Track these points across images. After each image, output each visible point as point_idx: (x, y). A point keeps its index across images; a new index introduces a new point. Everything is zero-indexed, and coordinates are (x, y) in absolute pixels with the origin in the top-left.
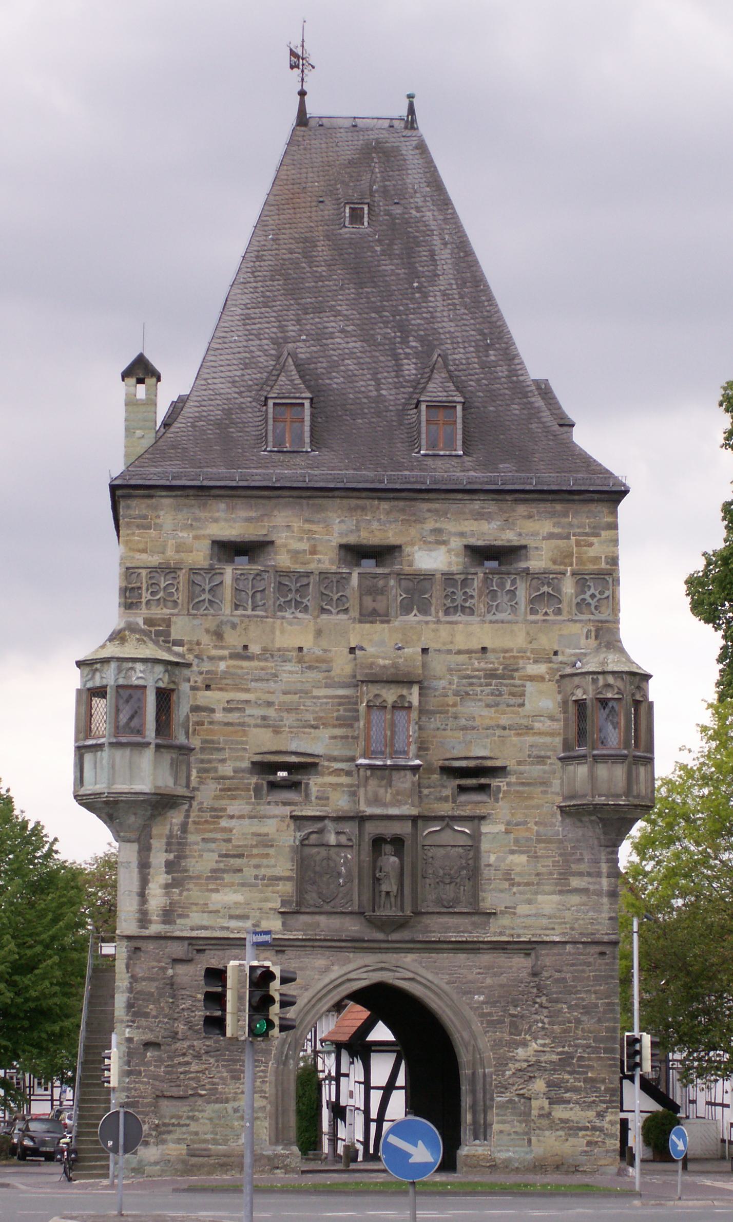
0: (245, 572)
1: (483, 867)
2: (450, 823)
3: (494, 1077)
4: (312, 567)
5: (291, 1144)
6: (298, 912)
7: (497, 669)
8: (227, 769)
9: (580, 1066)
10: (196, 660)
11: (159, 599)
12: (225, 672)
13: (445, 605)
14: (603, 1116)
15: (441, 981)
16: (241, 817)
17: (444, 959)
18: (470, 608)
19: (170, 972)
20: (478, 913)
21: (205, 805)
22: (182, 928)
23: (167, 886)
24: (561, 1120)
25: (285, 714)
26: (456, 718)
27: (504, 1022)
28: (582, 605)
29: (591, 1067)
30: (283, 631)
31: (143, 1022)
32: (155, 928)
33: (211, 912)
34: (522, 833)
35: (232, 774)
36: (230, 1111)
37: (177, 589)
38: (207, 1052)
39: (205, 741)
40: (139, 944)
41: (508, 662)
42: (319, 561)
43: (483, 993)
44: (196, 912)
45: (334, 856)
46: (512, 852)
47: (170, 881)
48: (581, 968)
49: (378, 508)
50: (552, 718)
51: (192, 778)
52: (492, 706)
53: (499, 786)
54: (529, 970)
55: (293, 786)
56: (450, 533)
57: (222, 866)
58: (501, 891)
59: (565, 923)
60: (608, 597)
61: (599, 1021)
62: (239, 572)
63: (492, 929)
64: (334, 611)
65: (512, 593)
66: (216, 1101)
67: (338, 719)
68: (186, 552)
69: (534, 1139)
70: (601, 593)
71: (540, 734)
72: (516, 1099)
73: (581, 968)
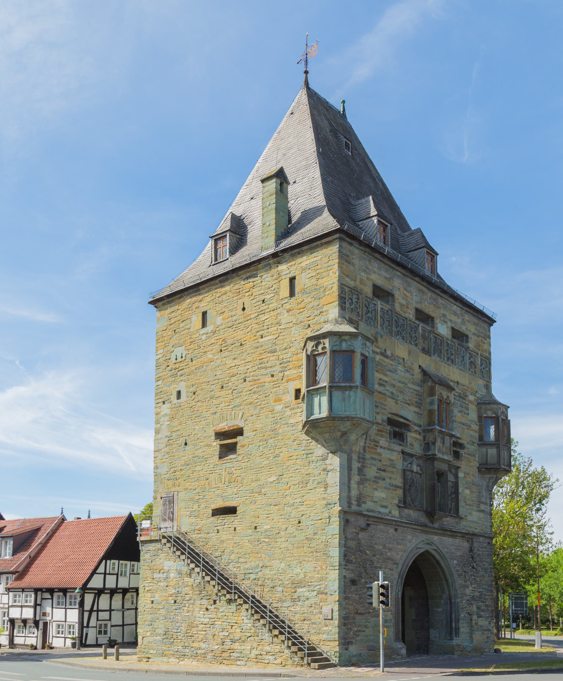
7: (461, 394)
16: (385, 448)
21: (372, 438)
25: (399, 393)
29: (487, 599)
32: (354, 508)
46: (466, 488)
47: (359, 480)
57: (378, 475)
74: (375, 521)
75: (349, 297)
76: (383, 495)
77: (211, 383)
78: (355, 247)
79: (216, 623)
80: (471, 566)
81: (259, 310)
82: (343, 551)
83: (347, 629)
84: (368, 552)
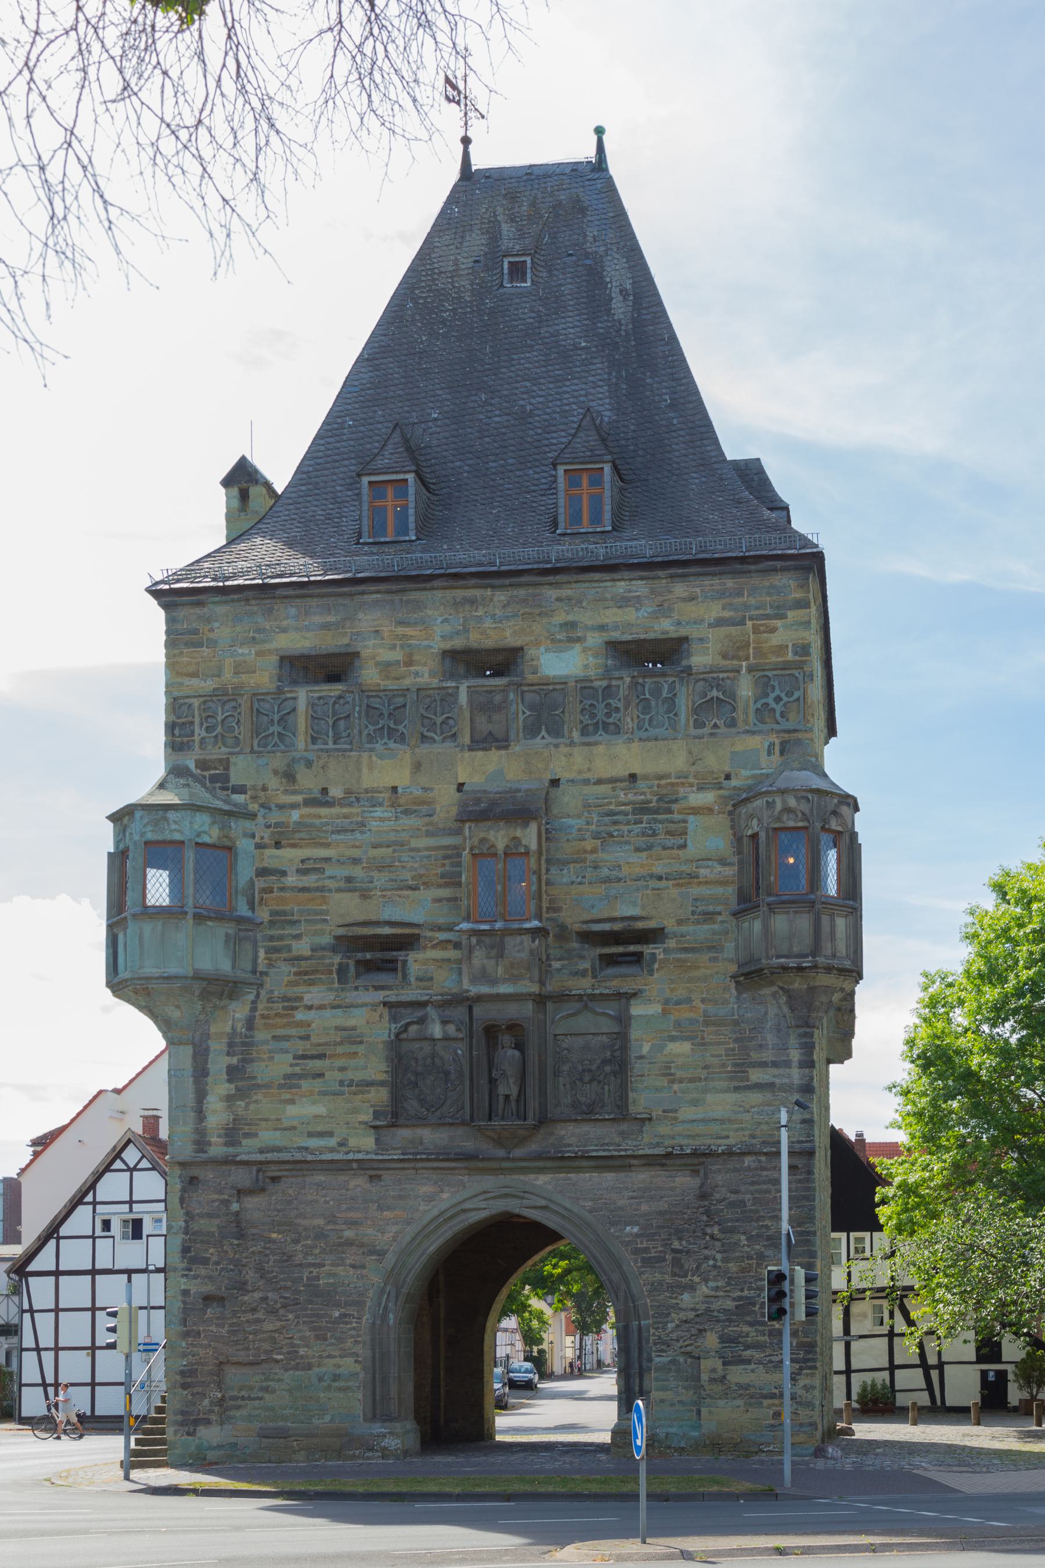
0: (323, 694)
1: (633, 1060)
2: (590, 1004)
3: (652, 1331)
4: (407, 682)
7: (650, 802)
8: (302, 947)
10: (262, 810)
12: (298, 823)
13: (581, 722)
16: (321, 1007)
17: (588, 1180)
18: (614, 723)
19: (235, 1207)
21: (276, 994)
22: (248, 1149)
23: (229, 1099)
24: (740, 1386)
25: (375, 874)
26: (595, 868)
27: (665, 1260)
28: (763, 713)
30: (371, 768)
31: (202, 1271)
33: (285, 1129)
34: (684, 1014)
35: (310, 953)
37: (239, 721)
39: (273, 913)
41: (664, 792)
42: (417, 674)
43: (637, 1224)
44: (267, 1129)
46: (673, 1039)
47: (233, 1092)
48: (764, 1187)
49: (491, 600)
50: (723, 862)
51: (260, 960)
52: (645, 850)
53: (654, 954)
55: (389, 966)
56: (587, 628)
57: (297, 1070)
58: (658, 1090)
59: (743, 1129)
60: (798, 699)
62: (316, 695)
64: (437, 738)
66: (296, 1368)
67: (443, 876)
68: (248, 672)
69: (704, 1411)
72: (681, 1359)
73: (764, 1187)
76: (320, 1109)
78: (214, 603)
83: (193, 1395)
84: (274, 1235)
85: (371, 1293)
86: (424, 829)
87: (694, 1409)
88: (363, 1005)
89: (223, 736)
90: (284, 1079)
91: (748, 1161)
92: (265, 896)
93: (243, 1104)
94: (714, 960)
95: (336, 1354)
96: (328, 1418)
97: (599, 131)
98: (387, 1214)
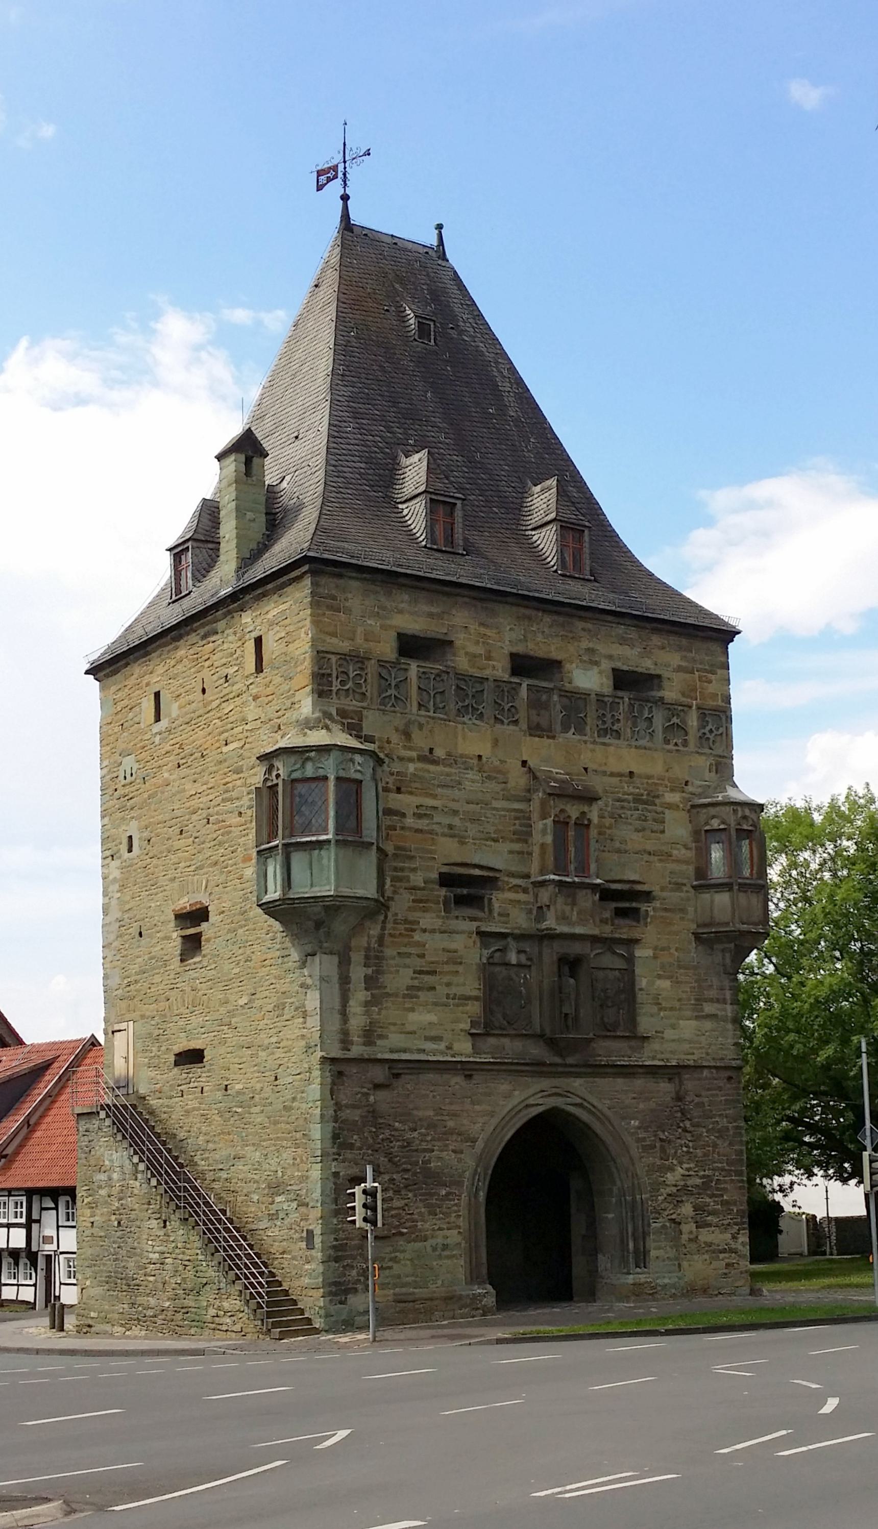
4: (487, 673)
5: (484, 1282)
6: (487, 1034)
7: (642, 795)
8: (417, 879)
9: (717, 1189)
11: (348, 690)
14: (737, 1238)
15: (602, 1105)
16: (433, 931)
17: (604, 1083)
20: (635, 1037)
21: (399, 917)
23: (367, 1004)
25: (468, 824)
27: (655, 1147)
29: (725, 1189)
31: (349, 1154)
32: (357, 1051)
35: (423, 885)
36: (429, 1249)
37: (365, 680)
38: (406, 1187)
39: (397, 848)
40: (342, 1067)
42: (494, 667)
44: (395, 1032)
45: (514, 976)
46: (659, 977)
47: (369, 999)
50: (686, 847)
51: (386, 887)
54: (673, 1095)
57: (416, 983)
59: (701, 1048)
60: (721, 734)
61: (730, 1144)
62: (422, 670)
63: (646, 1054)
64: (506, 721)
65: (650, 720)
69: (685, 1264)
70: (717, 729)
71: (678, 861)
72: (668, 1224)
74: (408, 1068)
75: (340, 670)
76: (432, 1018)
77: (168, 824)
79: (167, 1260)
80: (680, 1127)
81: (222, 695)
82: (330, 1129)
85: (467, 1174)
86: (502, 793)
87: (676, 1263)
88: (462, 932)
89: (354, 691)
90: (407, 990)
91: (706, 1073)
92: (390, 832)
93: (376, 1009)
94: (682, 919)
95: (445, 1227)
96: (440, 1282)
97: (440, 227)
98: (477, 1107)
